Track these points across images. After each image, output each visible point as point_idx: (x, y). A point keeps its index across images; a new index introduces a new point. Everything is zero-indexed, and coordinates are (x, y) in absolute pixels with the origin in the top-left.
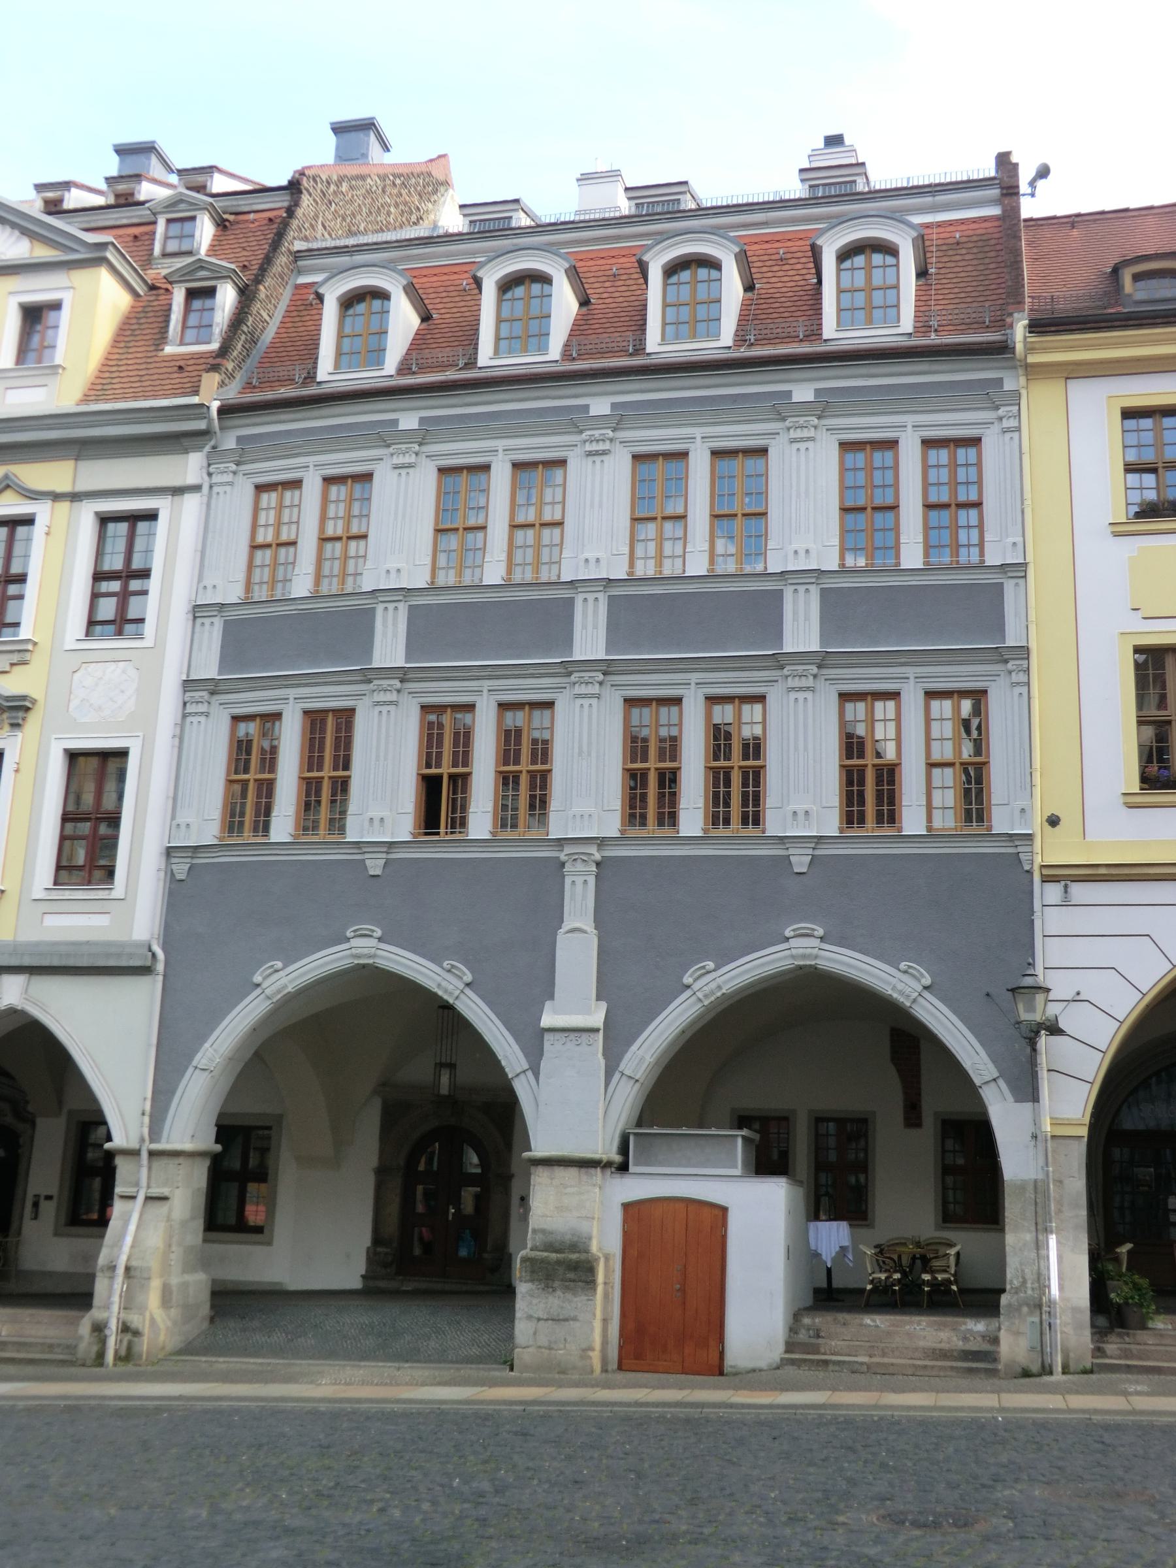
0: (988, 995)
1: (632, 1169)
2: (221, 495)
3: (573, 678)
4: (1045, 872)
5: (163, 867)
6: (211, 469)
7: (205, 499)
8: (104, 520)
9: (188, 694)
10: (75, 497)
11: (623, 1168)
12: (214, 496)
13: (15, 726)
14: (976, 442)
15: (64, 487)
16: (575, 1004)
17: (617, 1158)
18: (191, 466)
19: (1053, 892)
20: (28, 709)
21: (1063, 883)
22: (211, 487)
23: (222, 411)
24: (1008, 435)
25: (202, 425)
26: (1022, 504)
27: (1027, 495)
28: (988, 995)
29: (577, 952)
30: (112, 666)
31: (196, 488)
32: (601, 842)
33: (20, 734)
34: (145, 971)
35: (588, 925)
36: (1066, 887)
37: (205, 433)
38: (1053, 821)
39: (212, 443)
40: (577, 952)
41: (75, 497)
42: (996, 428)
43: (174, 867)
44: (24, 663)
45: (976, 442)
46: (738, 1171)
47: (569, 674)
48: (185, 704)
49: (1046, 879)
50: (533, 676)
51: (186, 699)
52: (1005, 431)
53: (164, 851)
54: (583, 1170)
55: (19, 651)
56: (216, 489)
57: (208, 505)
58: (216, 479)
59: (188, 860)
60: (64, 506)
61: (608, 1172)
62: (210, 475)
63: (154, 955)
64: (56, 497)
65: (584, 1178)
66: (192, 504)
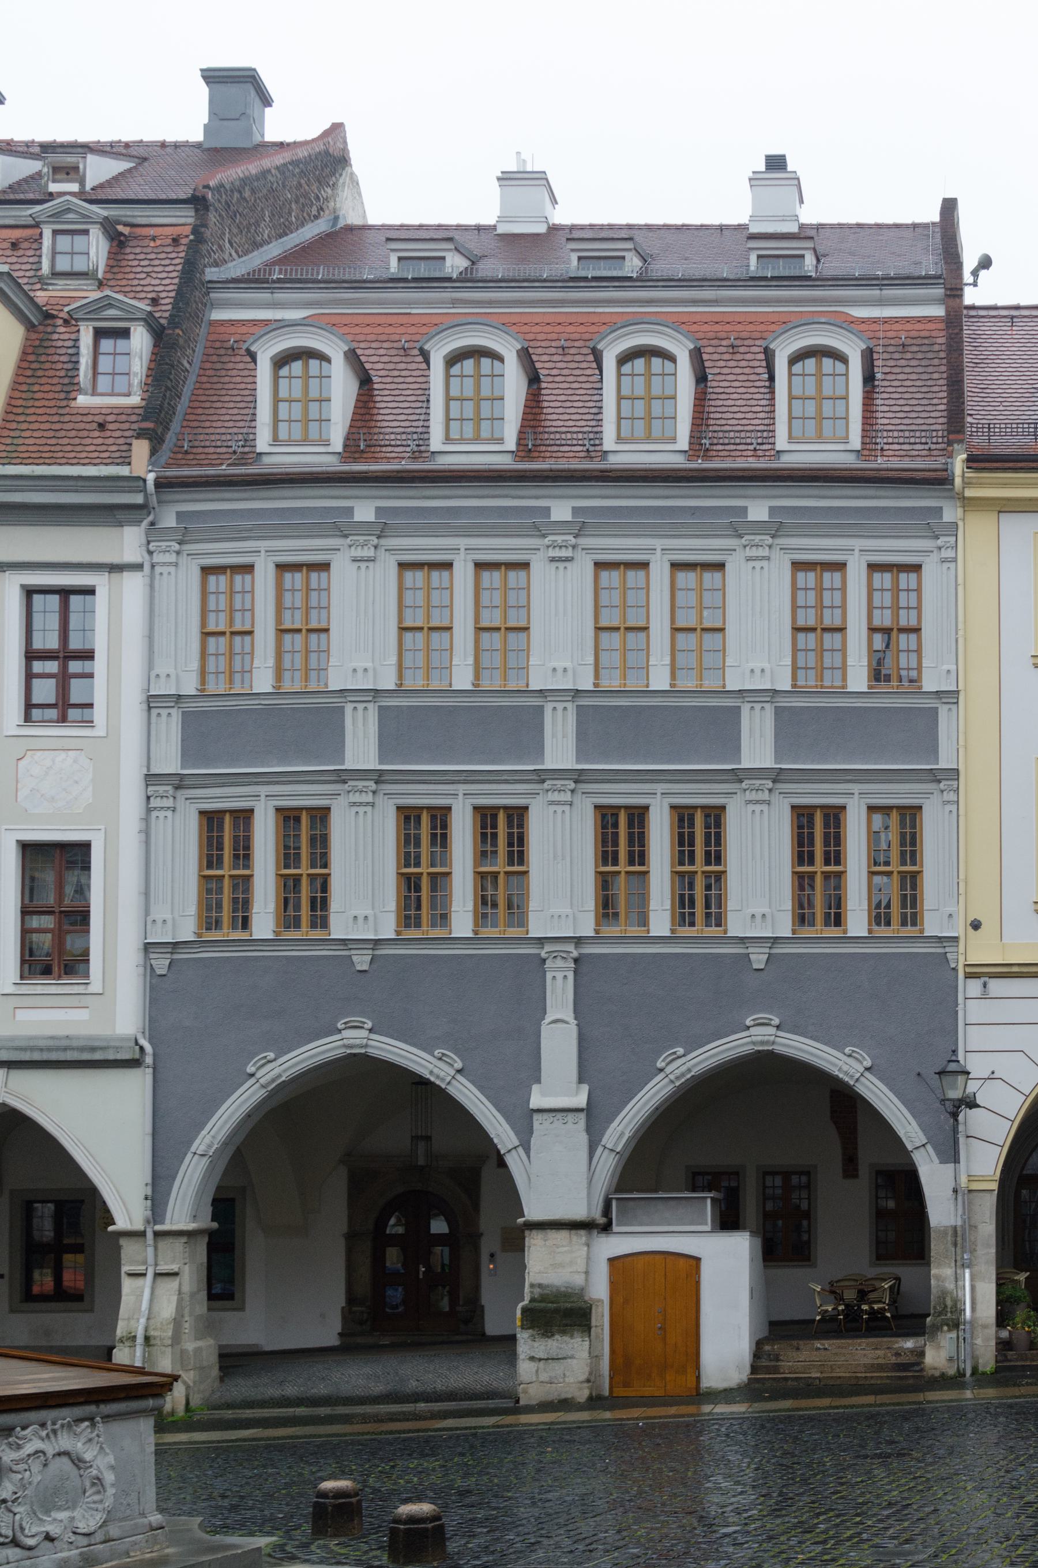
0: (919, 1074)
1: (615, 1228)
2: (165, 575)
3: (546, 785)
4: (968, 970)
5: (142, 962)
6: (152, 547)
11: (606, 1228)
12: (157, 577)
14: (917, 568)
17: (602, 1221)
19: (974, 987)
21: (983, 979)
22: (153, 566)
23: (159, 484)
24: (946, 565)
26: (957, 634)
27: (961, 626)
28: (919, 1074)
32: (578, 941)
36: (985, 985)
37: (143, 508)
38: (976, 925)
39: (151, 518)
42: (935, 557)
43: (153, 962)
45: (917, 568)
46: (708, 1228)
47: (543, 781)
49: (968, 976)
50: (506, 782)
52: (944, 561)
53: (142, 947)
54: (573, 1232)
56: (158, 569)
57: (152, 586)
58: (157, 558)
61: (595, 1232)
65: (574, 1238)
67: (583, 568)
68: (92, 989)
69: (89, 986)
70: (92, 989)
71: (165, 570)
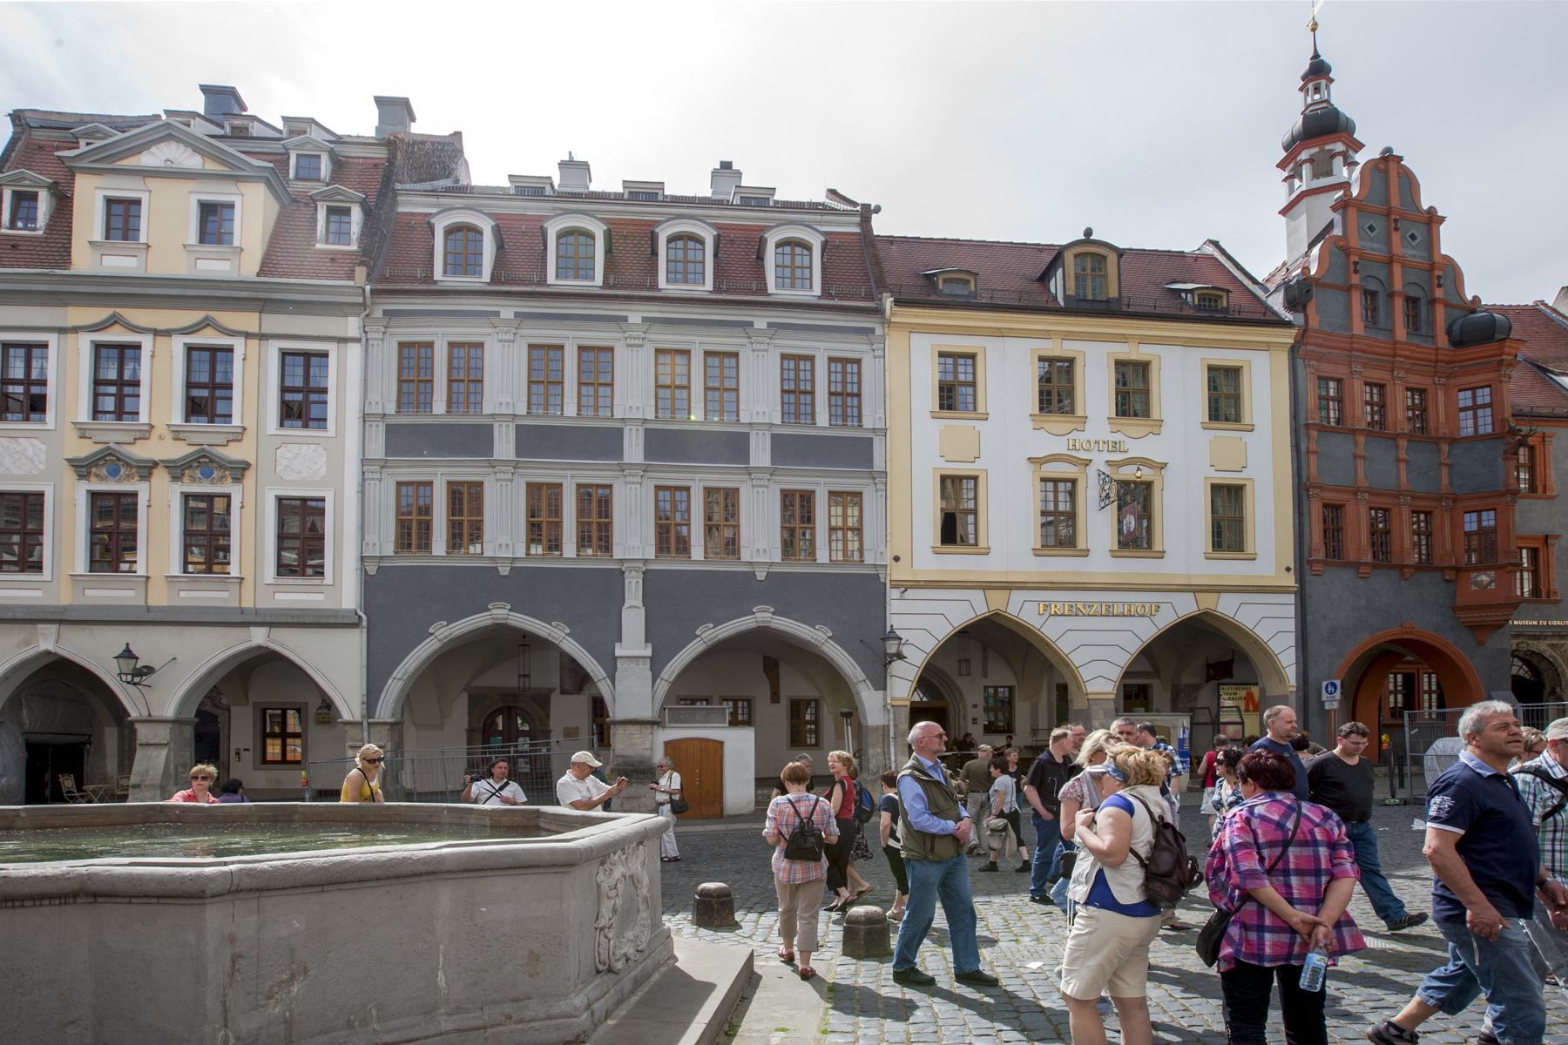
8: (284, 354)
10: (263, 337)
16: (633, 641)
29: (633, 619)
31: (358, 340)
35: (639, 603)
40: (633, 619)
41: (263, 337)
60: (254, 343)
67: (648, 353)
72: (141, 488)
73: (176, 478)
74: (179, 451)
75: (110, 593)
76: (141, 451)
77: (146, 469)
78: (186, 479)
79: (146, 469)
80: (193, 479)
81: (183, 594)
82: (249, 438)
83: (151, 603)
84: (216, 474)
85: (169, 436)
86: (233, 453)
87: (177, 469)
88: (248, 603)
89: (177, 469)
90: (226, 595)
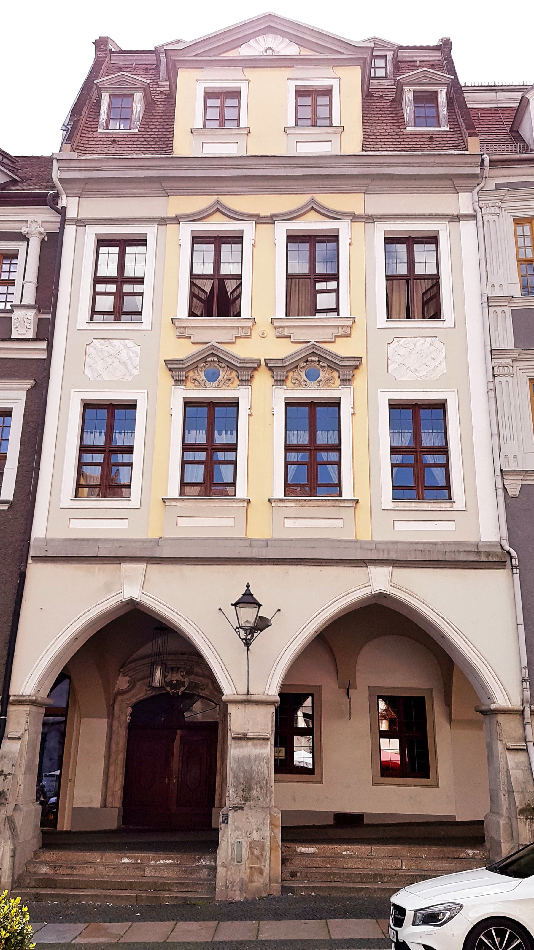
2: (491, 222)
7: (480, 224)
9: (494, 361)
10: (370, 219)
12: (485, 223)
13: (347, 381)
15: (359, 211)
18: (464, 202)
20: (356, 367)
25: (477, 171)
30: (422, 340)
33: (352, 387)
34: (499, 564)
44: (349, 336)
48: (493, 368)
51: (494, 365)
55: (343, 326)
59: (519, 482)
60: (359, 226)
62: (481, 208)
63: (508, 552)
64: (354, 217)
66: (468, 228)
68: (456, 506)
69: (454, 504)
70: (456, 506)
71: (491, 219)
72: (242, 394)
73: (280, 382)
74: (282, 350)
75: (208, 523)
76: (242, 351)
77: (246, 371)
78: (289, 382)
79: (246, 371)
80: (297, 383)
81: (289, 523)
82: (358, 332)
83: (251, 536)
84: (323, 375)
85: (271, 333)
86: (342, 349)
87: (279, 371)
88: (364, 536)
89: (279, 371)
90: (338, 523)
